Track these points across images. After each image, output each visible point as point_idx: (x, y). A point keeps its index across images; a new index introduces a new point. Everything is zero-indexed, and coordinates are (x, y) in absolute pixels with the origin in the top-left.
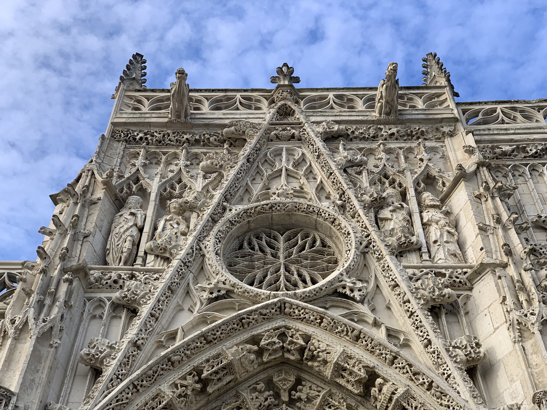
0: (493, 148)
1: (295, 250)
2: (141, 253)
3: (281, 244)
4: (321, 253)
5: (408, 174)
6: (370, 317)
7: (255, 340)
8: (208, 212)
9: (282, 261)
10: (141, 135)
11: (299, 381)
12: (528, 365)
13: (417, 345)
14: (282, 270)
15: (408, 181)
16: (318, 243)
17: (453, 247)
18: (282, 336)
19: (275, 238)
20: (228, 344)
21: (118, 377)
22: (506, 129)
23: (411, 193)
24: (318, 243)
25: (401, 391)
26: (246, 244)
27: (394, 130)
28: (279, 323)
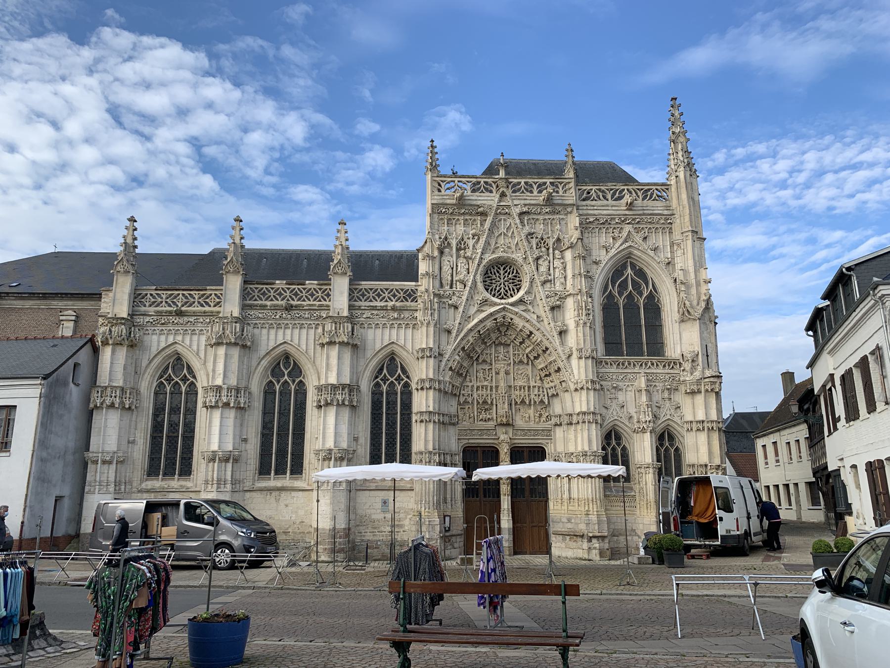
0: (586, 219)
1: (506, 274)
2: (454, 282)
3: (502, 272)
4: (516, 277)
5: (551, 239)
6: (532, 311)
7: (496, 319)
8: (477, 262)
9: (502, 281)
10: (444, 210)
11: (508, 329)
12: (577, 336)
13: (546, 322)
14: (502, 285)
15: (551, 242)
16: (515, 271)
17: (563, 280)
18: (504, 318)
19: (499, 268)
20: (488, 321)
21: (457, 336)
22: (594, 206)
23: (551, 250)
24: (515, 271)
25: (539, 339)
26: (489, 272)
27: (547, 210)
28: (503, 313)
